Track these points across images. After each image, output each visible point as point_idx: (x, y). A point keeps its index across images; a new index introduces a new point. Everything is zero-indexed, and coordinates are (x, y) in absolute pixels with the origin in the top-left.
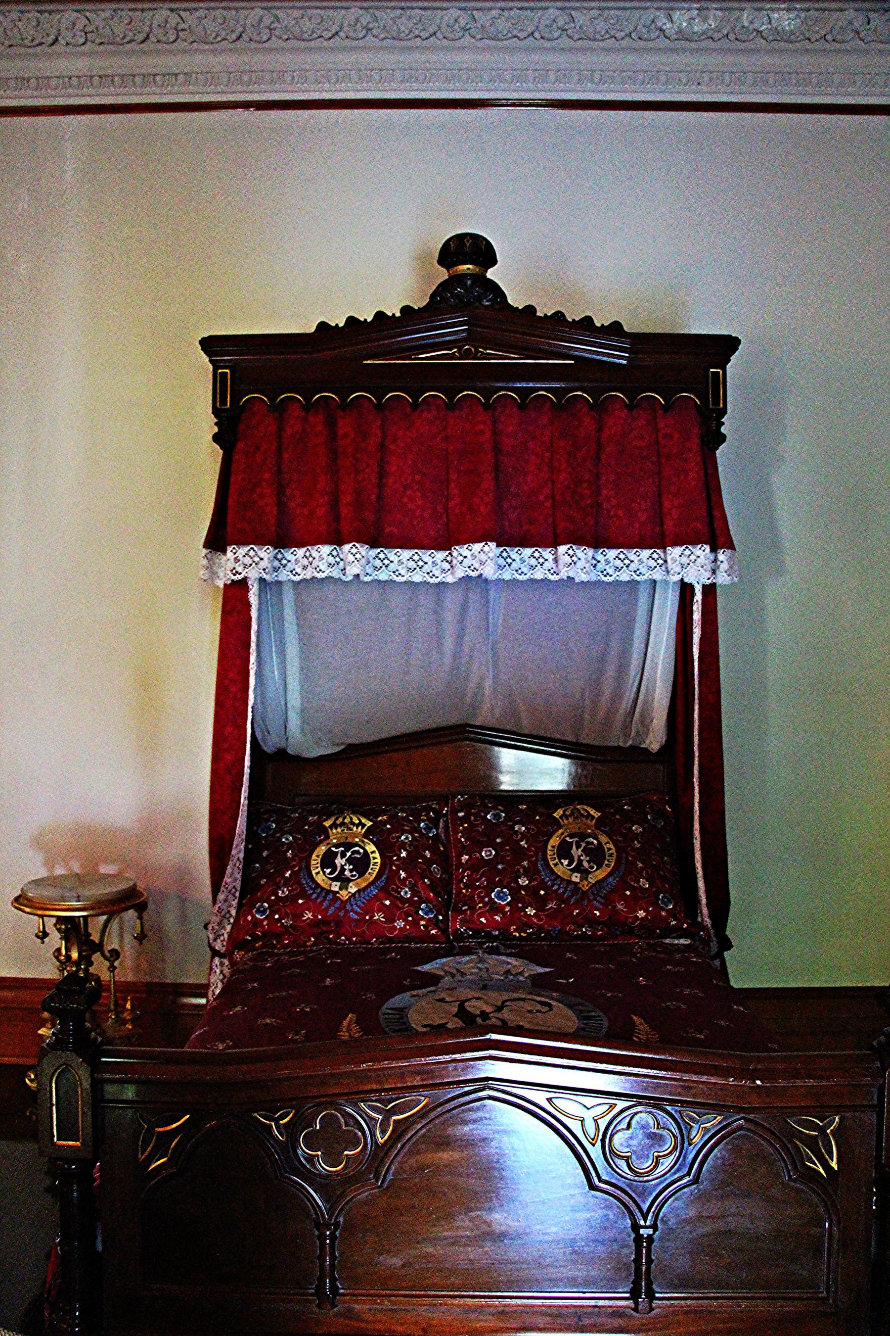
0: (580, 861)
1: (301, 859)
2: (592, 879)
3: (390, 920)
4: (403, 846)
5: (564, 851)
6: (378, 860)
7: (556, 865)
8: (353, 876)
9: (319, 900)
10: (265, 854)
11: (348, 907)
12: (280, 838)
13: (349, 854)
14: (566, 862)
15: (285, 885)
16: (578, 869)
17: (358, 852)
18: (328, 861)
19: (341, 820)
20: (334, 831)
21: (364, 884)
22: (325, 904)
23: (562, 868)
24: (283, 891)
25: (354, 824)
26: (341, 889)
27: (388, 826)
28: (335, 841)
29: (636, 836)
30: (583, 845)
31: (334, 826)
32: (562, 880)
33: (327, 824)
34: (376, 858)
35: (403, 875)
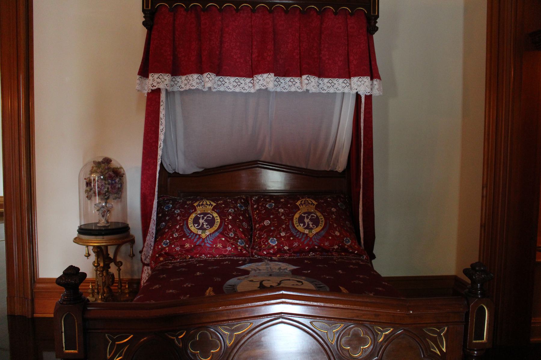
0: (308, 224)
1: (184, 220)
2: (314, 232)
3: (224, 247)
5: (301, 220)
6: (219, 220)
10: (167, 218)
11: (206, 241)
12: (174, 211)
13: (205, 218)
14: (302, 225)
15: (176, 232)
16: (308, 228)
17: (210, 217)
19: (202, 203)
21: (213, 231)
22: (195, 240)
23: (300, 228)
25: (207, 204)
26: (202, 233)
29: (333, 213)
30: (310, 217)
31: (199, 205)
32: (301, 232)
33: (195, 205)
34: (218, 220)
35: (230, 227)
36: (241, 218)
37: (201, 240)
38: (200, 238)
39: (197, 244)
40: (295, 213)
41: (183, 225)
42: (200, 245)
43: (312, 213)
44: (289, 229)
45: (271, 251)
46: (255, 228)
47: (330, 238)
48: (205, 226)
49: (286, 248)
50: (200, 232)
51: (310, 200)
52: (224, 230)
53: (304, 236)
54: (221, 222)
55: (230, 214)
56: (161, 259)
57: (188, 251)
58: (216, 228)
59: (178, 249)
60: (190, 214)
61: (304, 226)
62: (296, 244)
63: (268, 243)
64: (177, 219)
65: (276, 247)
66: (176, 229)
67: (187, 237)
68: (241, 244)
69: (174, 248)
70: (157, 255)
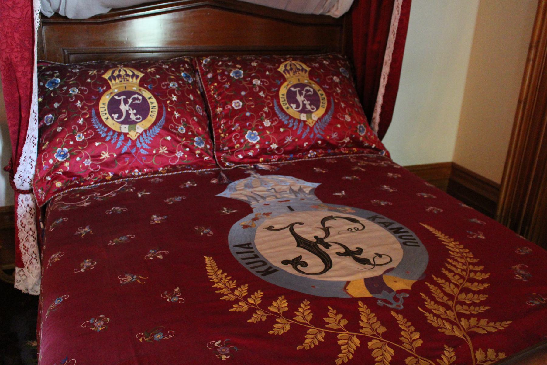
0: (304, 105)
1: (90, 108)
3: (172, 152)
5: (291, 97)
6: (156, 104)
7: (288, 108)
8: (137, 119)
9: (113, 142)
10: (56, 105)
11: (138, 145)
12: (67, 91)
13: (130, 101)
14: (294, 106)
16: (304, 110)
17: (138, 99)
18: (114, 107)
20: (113, 82)
21: (149, 125)
22: (119, 145)
23: (292, 110)
24: (80, 136)
25: (127, 75)
27: (158, 76)
28: (116, 91)
29: (336, 85)
30: (304, 92)
31: (113, 77)
32: (295, 119)
33: (106, 76)
34: (153, 103)
35: (177, 115)
37: (129, 143)
38: (127, 139)
39: (124, 150)
40: (279, 87)
41: (91, 117)
42: (128, 153)
43: (305, 85)
44: (275, 115)
45: (251, 154)
46: (216, 115)
47: (339, 126)
48: (133, 117)
49: (274, 146)
50: (125, 129)
51: (299, 64)
52: (168, 121)
53: (302, 125)
54: (160, 107)
55: (172, 91)
56: (58, 184)
57: (108, 164)
58: (153, 120)
59: (88, 162)
60: (100, 96)
61: (298, 107)
62: (289, 139)
63: (245, 140)
64: (76, 107)
65: (257, 146)
66: (79, 125)
67: (103, 140)
68: (199, 144)
69: (81, 162)
70: (49, 178)
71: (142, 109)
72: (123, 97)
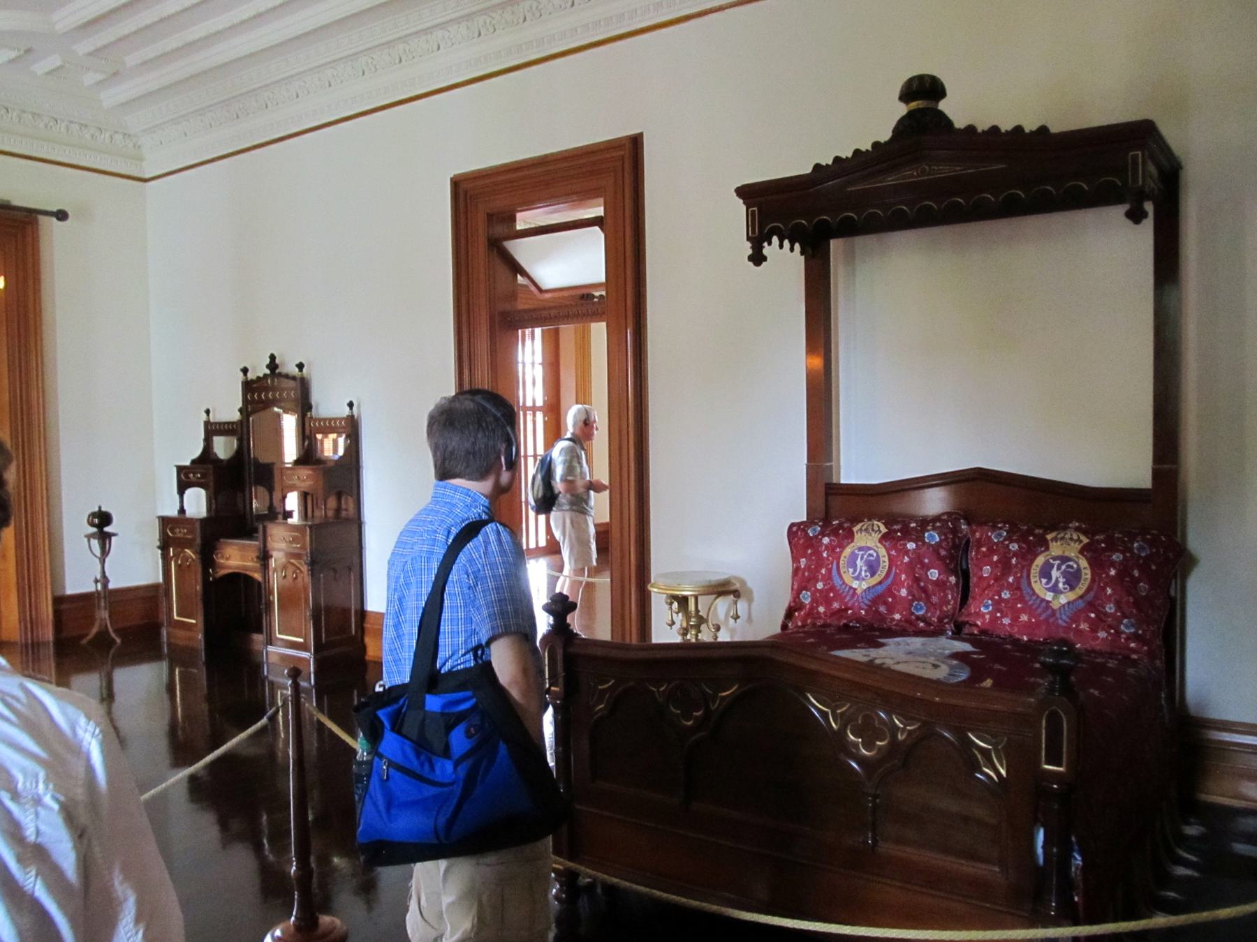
1: (1023, 567)
3: (1094, 630)
4: (1113, 564)
6: (1089, 576)
11: (1058, 615)
13: (1063, 567)
18: (1045, 573)
25: (1071, 539)
31: (1055, 539)
33: (1049, 537)
34: (1087, 574)
35: (1109, 591)
36: (1136, 573)
37: (1049, 612)
48: (1061, 585)
54: (1093, 580)
71: (1072, 579)
72: (1057, 562)
